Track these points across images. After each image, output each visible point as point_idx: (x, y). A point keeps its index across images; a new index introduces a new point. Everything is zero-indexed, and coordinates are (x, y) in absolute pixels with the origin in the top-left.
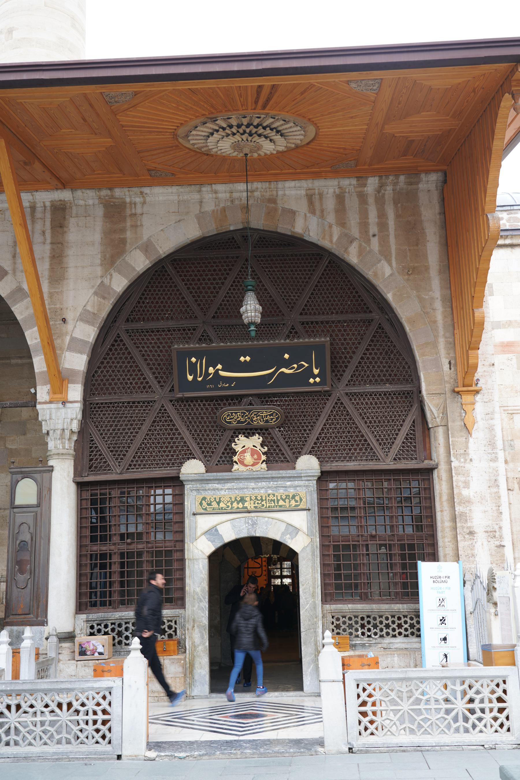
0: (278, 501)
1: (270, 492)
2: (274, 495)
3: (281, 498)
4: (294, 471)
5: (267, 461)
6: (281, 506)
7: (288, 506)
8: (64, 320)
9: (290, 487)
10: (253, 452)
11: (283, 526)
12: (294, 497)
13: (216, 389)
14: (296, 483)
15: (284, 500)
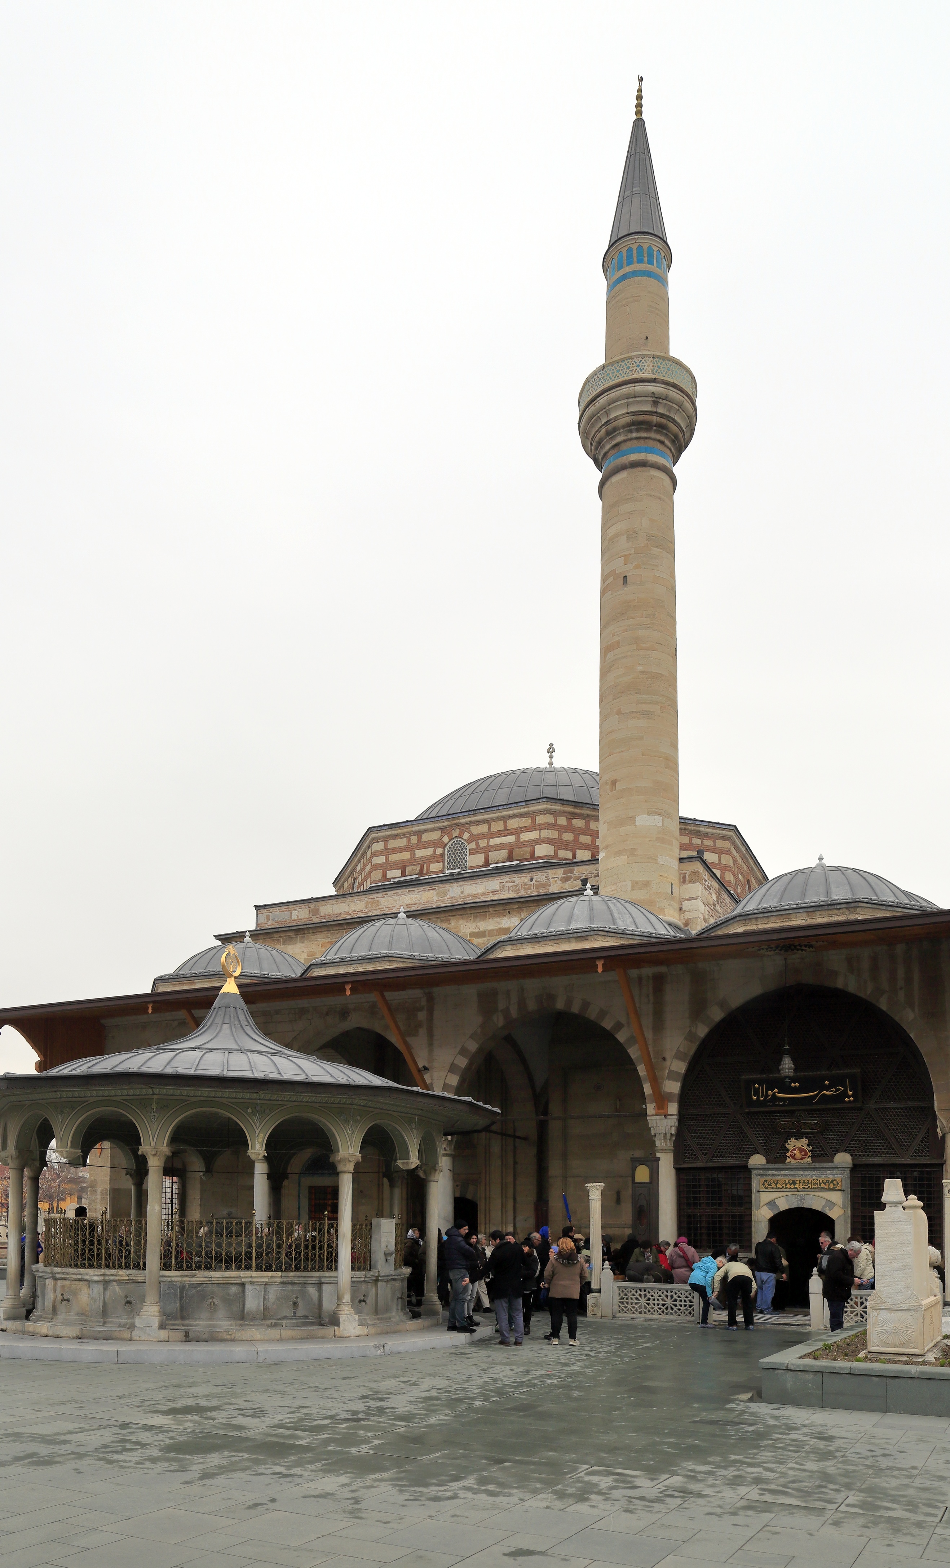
0: (820, 1184)
1: (814, 1177)
2: (817, 1180)
3: (823, 1182)
4: (832, 1164)
5: (812, 1157)
6: (822, 1188)
7: (827, 1187)
8: (664, 1059)
9: (830, 1174)
10: (802, 1150)
11: (823, 1202)
12: (832, 1181)
13: (774, 1105)
14: (834, 1172)
15: (825, 1184)
